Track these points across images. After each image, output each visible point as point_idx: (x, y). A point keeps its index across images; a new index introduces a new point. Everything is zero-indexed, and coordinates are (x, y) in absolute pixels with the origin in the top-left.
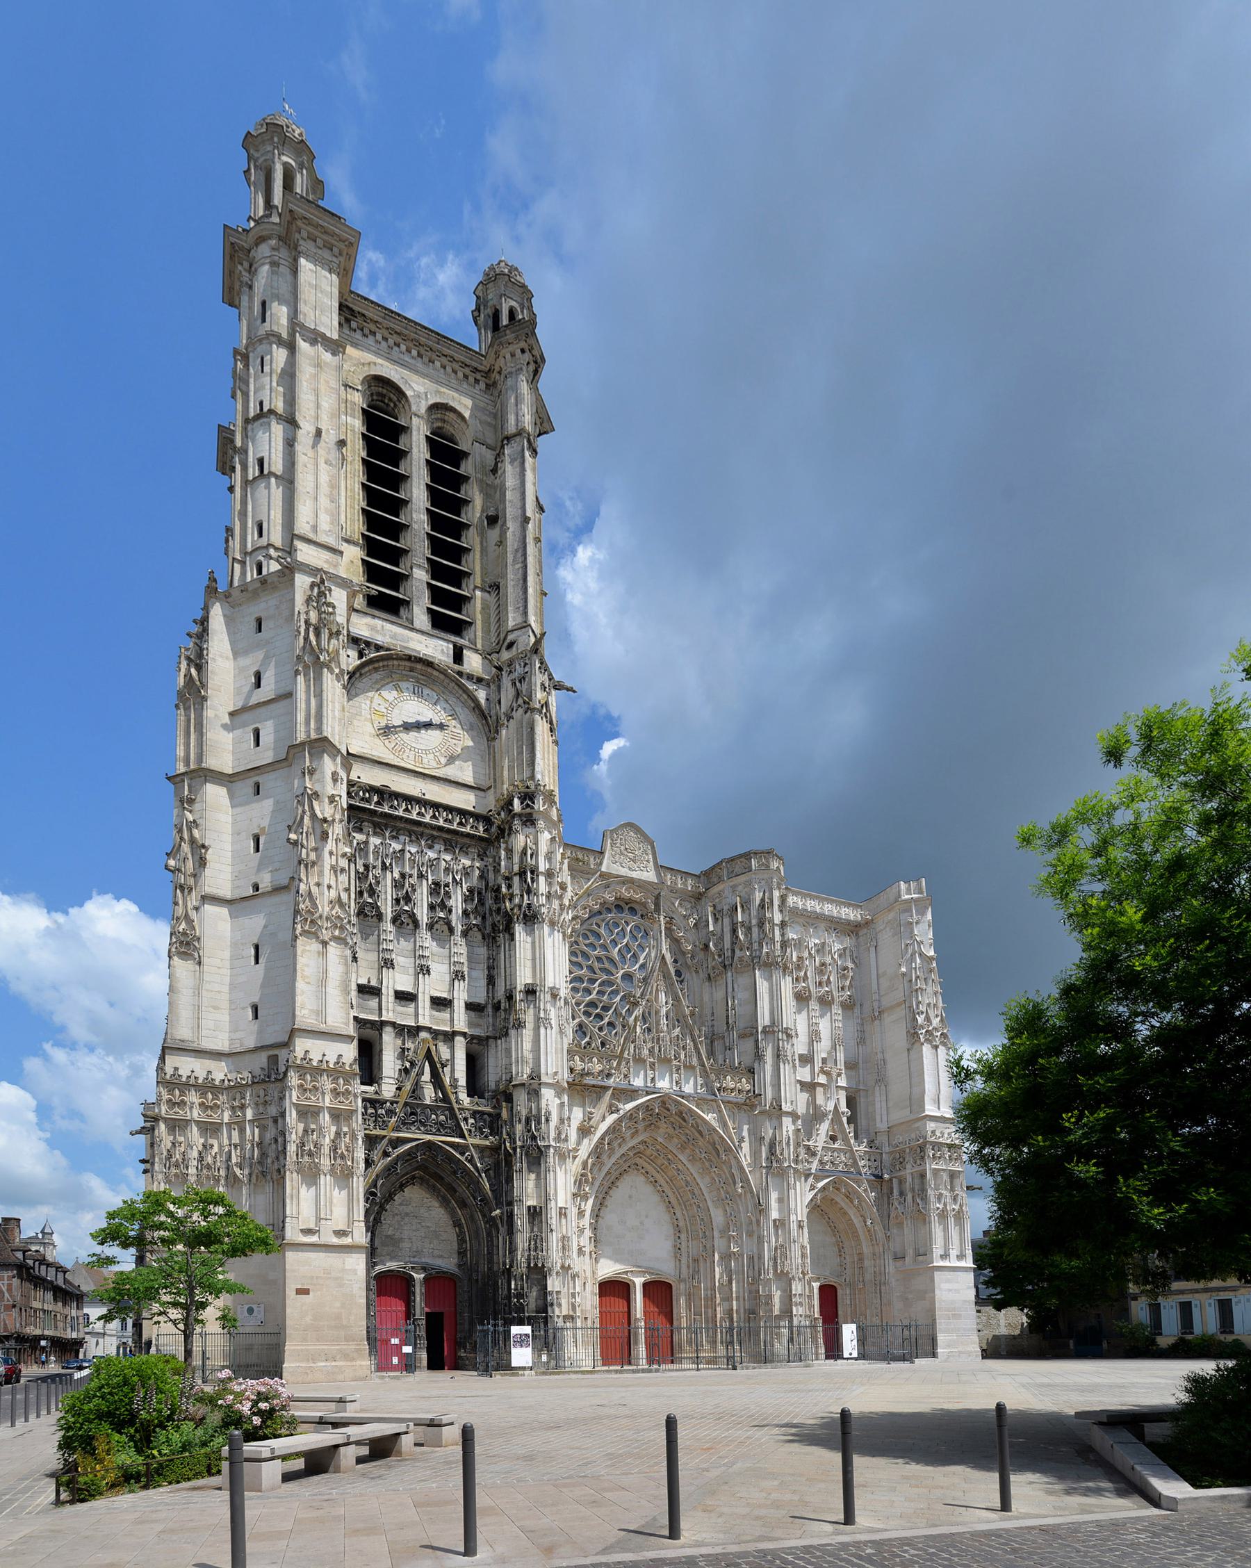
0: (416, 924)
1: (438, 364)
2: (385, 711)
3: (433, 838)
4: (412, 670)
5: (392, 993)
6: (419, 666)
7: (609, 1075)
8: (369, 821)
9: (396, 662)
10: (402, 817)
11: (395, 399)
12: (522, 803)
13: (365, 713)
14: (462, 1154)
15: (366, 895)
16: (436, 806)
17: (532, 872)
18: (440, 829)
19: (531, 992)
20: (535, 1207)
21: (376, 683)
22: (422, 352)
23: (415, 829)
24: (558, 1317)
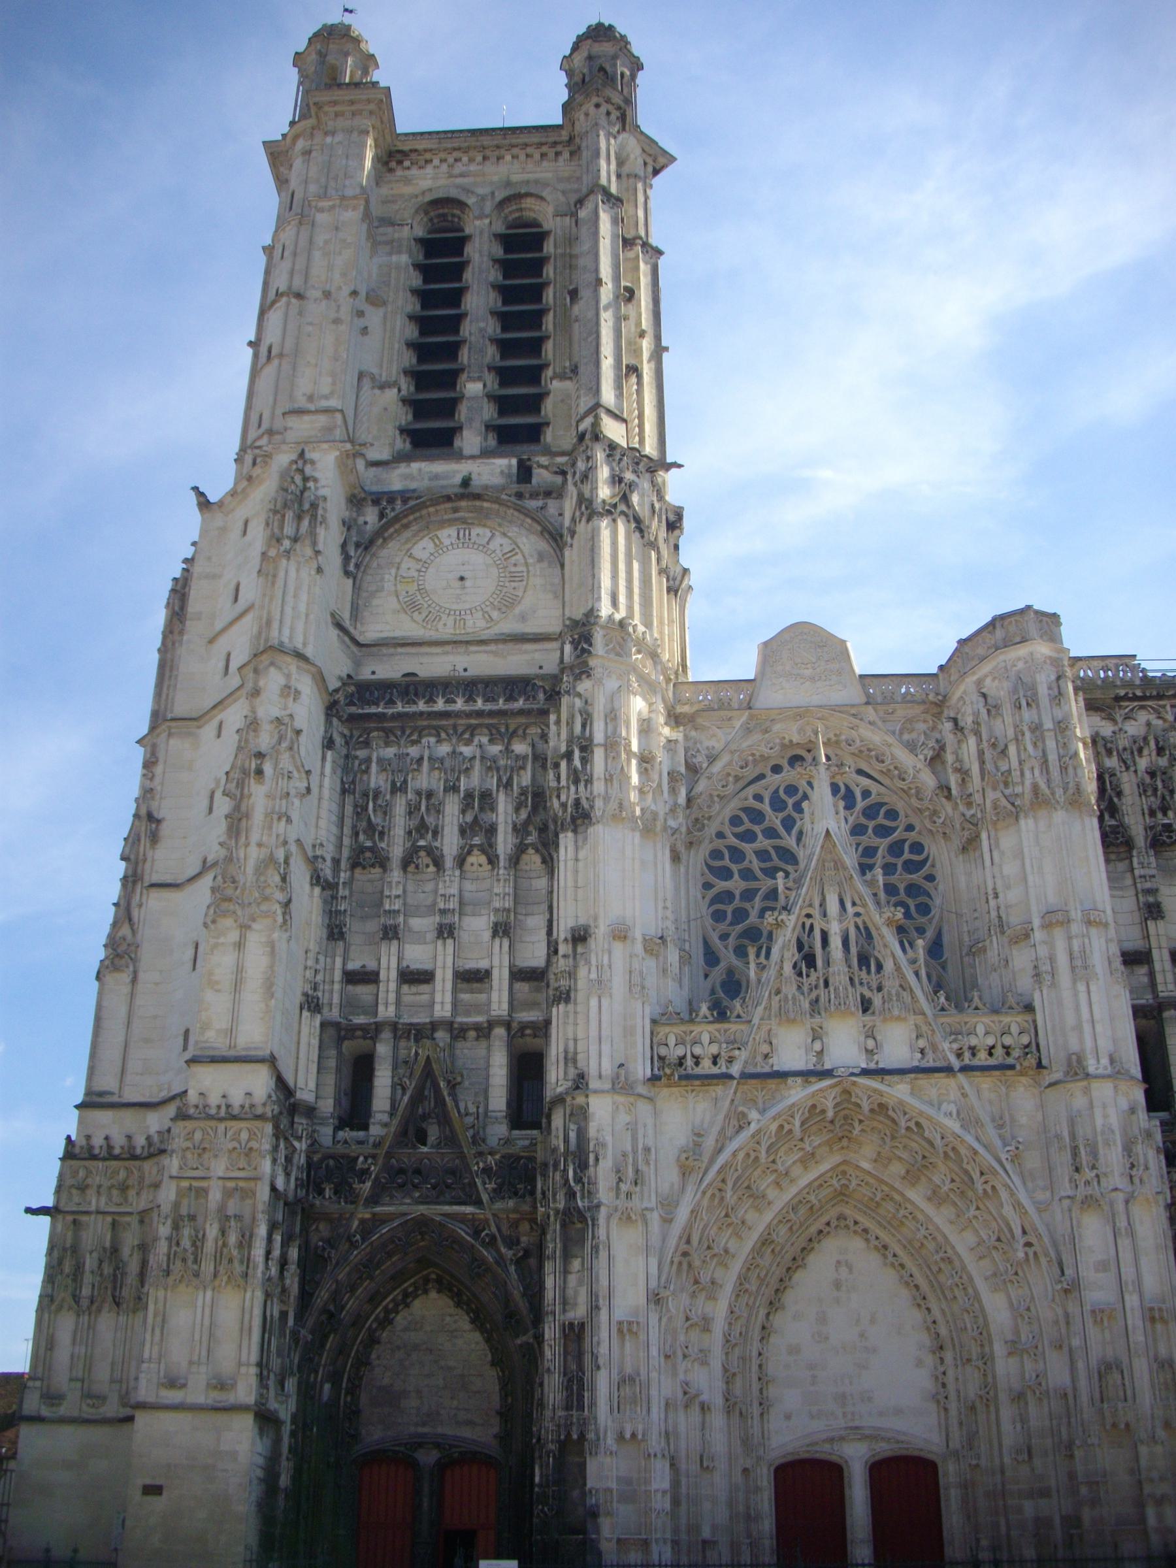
0: (438, 863)
1: (508, 158)
2: (416, 574)
3: (472, 730)
4: (456, 510)
5: (394, 974)
6: (463, 504)
7: (730, 1060)
8: (377, 729)
9: (431, 509)
10: (422, 713)
11: (457, 212)
12: (576, 649)
13: (389, 586)
14: (476, 1233)
15: (362, 837)
16: (471, 686)
17: (583, 749)
18: (480, 714)
19: (580, 937)
20: (571, 1324)
21: (406, 542)
22: (488, 153)
23: (444, 722)
24: (609, 1540)
